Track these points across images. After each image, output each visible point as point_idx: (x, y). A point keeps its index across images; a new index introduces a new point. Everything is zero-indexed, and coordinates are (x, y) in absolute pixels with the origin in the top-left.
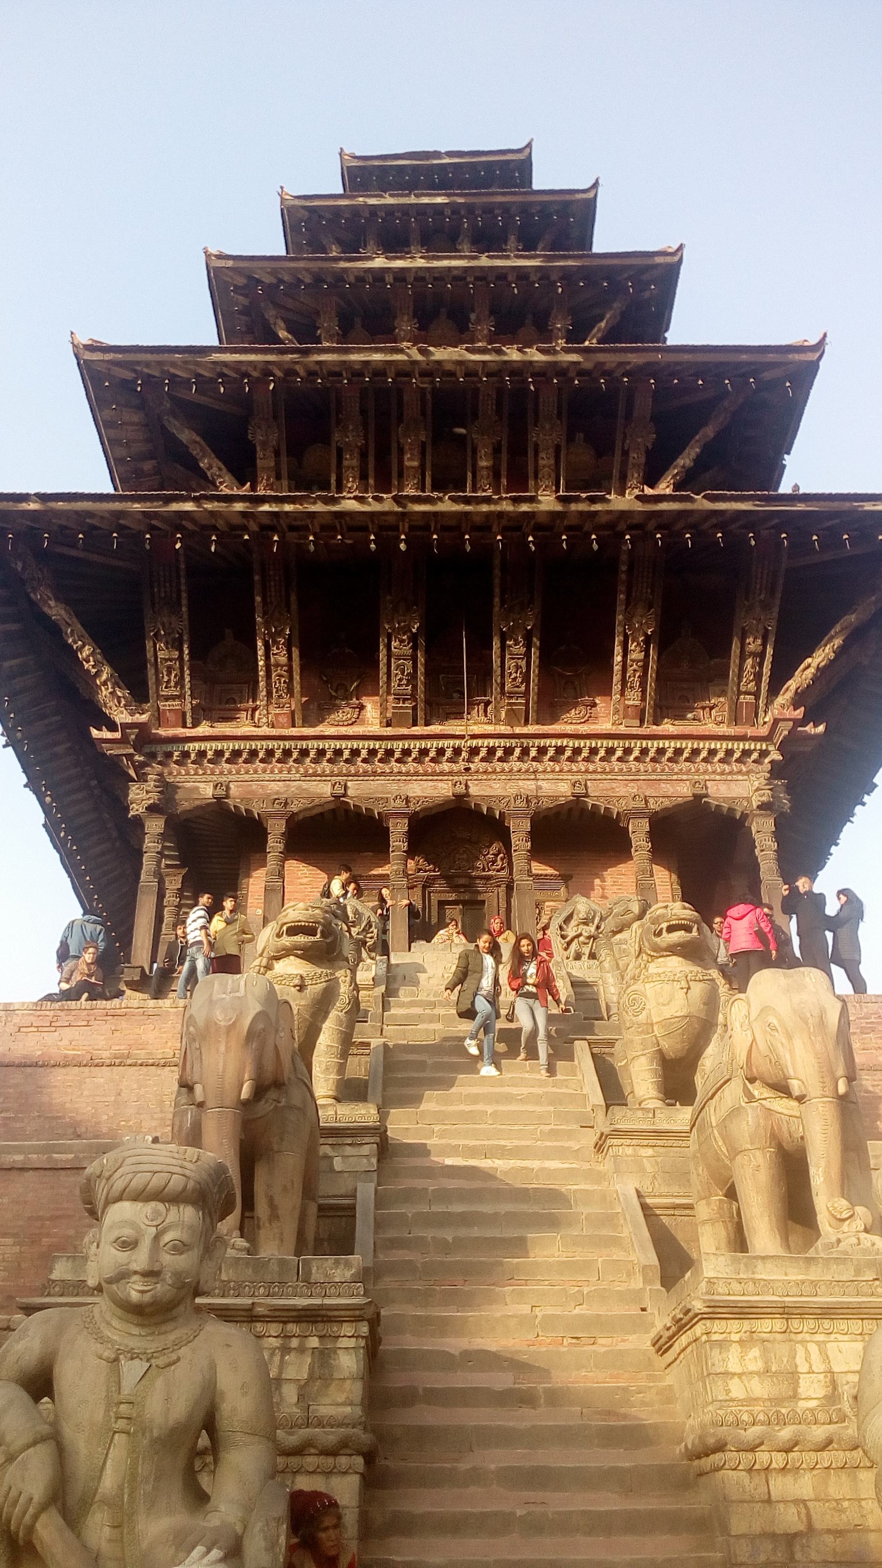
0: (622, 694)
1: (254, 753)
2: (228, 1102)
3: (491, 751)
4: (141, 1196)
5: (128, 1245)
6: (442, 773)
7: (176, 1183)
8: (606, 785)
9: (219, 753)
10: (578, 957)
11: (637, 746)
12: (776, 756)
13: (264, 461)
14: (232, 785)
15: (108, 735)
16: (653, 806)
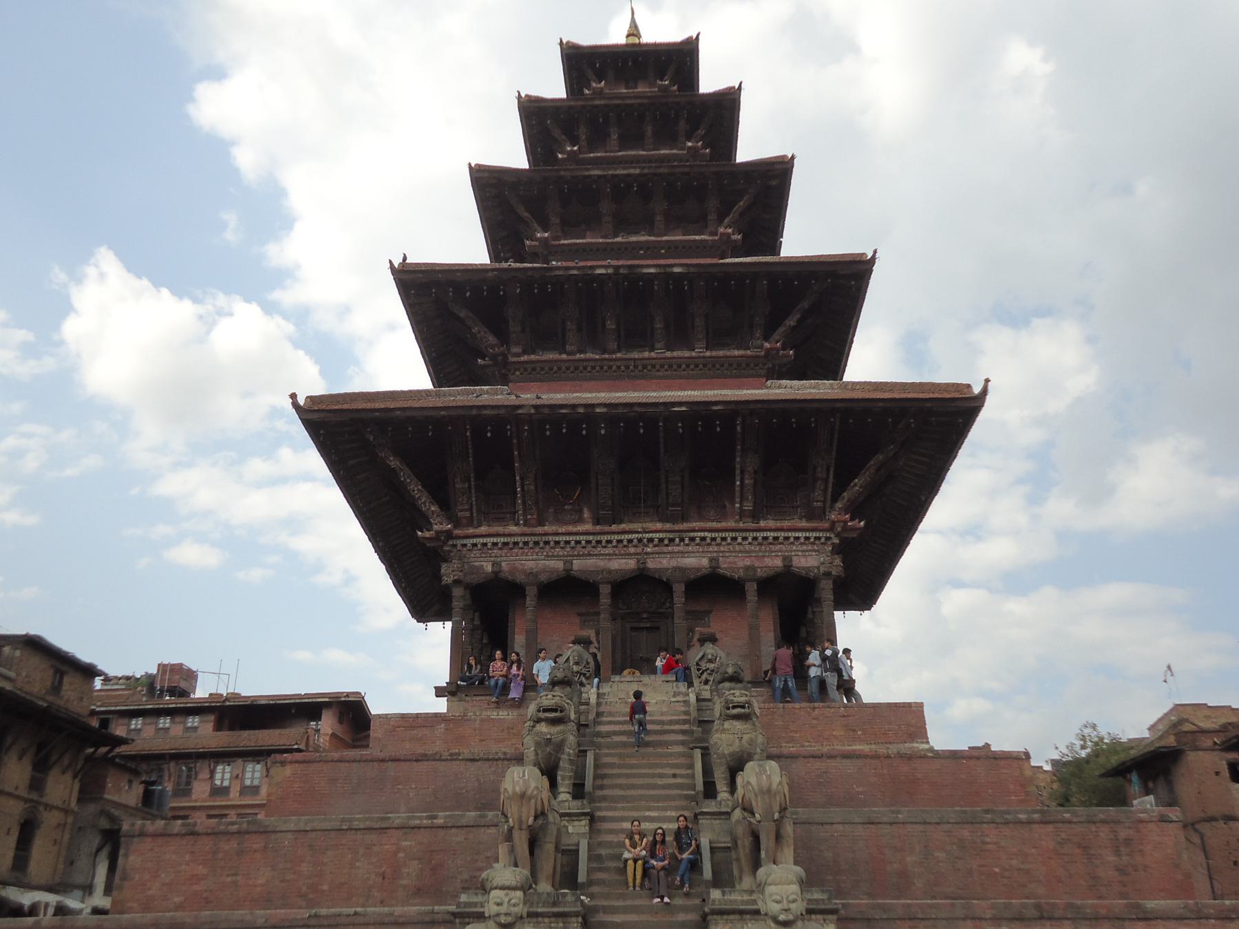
0: (741, 503)
1: (516, 544)
2: (524, 827)
3: (661, 540)
4: (503, 888)
5: (498, 904)
6: (630, 554)
7: (514, 883)
8: (731, 559)
9: (495, 544)
10: (706, 682)
11: (751, 535)
12: (836, 541)
13: (514, 327)
14: (503, 564)
15: (427, 534)
16: (759, 573)
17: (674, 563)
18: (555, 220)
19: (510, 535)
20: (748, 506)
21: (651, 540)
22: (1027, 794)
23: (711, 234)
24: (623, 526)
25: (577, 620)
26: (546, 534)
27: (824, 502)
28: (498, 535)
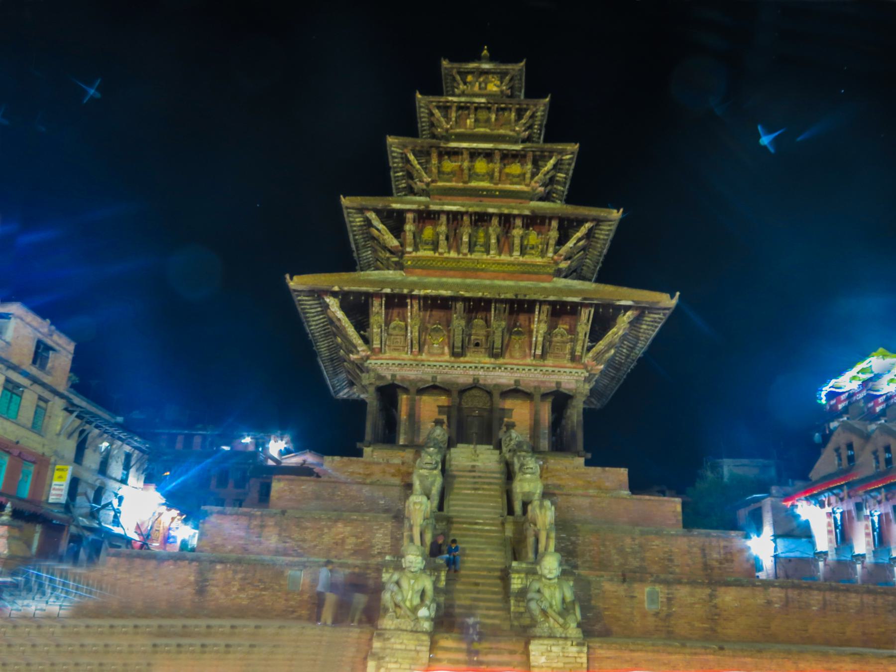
11: (539, 369)
12: (587, 374)
13: (409, 237)
16: (543, 390)
17: (494, 382)
18: (435, 170)
19: (403, 360)
20: (539, 352)
21: (482, 368)
22: (677, 520)
23: (527, 185)
24: (466, 359)
25: (437, 410)
26: (423, 361)
27: (582, 353)
28: (395, 359)
